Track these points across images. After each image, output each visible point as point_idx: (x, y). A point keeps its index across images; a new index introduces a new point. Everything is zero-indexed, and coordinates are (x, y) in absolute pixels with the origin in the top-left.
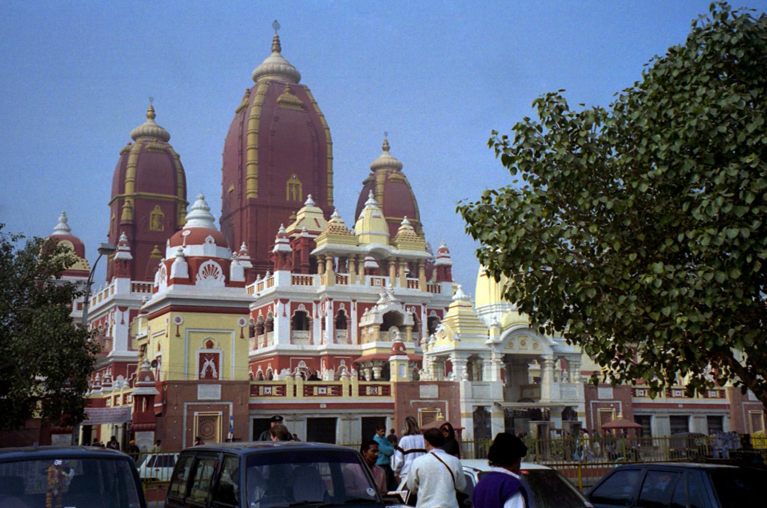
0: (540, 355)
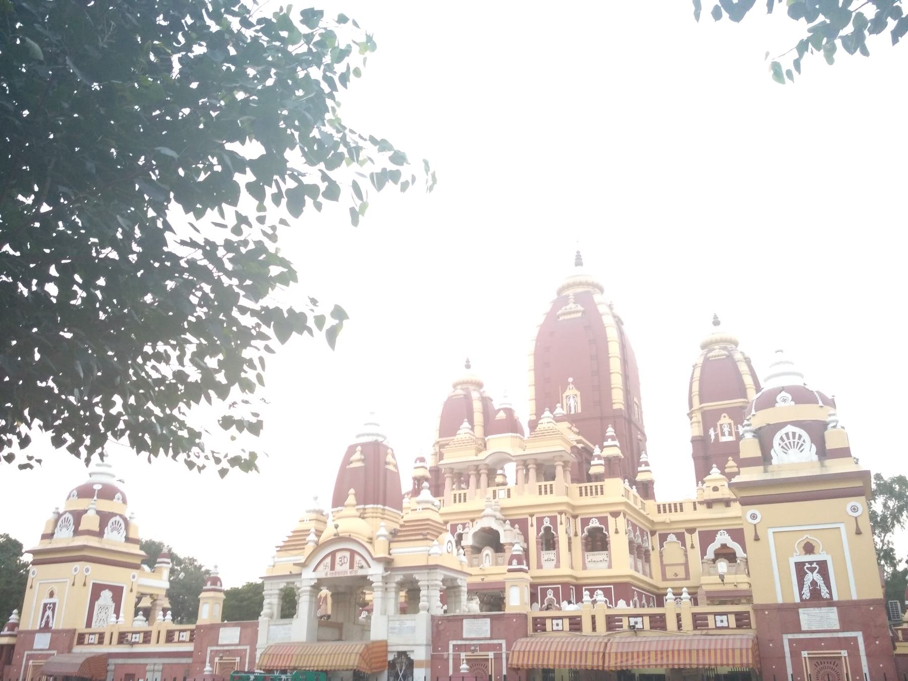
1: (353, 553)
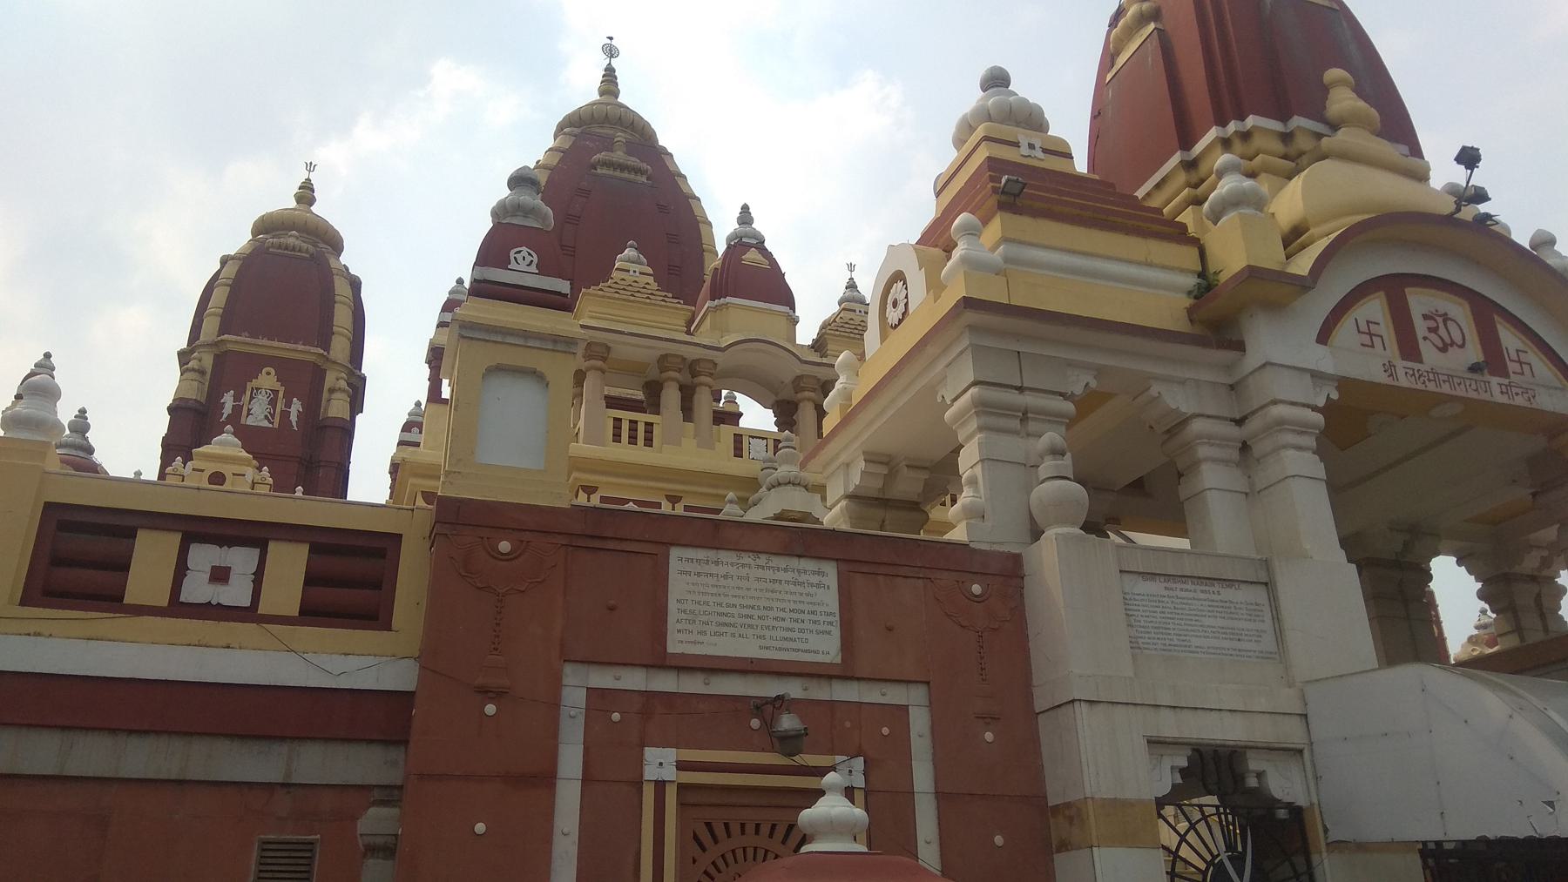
1: (1485, 311)
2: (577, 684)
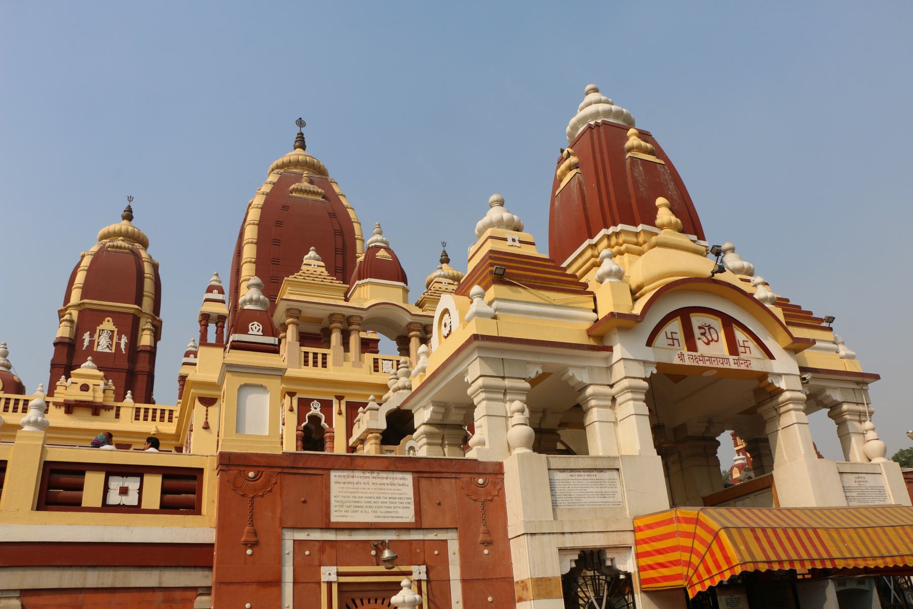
0: (763, 376)
1: (729, 323)
2: (290, 538)
